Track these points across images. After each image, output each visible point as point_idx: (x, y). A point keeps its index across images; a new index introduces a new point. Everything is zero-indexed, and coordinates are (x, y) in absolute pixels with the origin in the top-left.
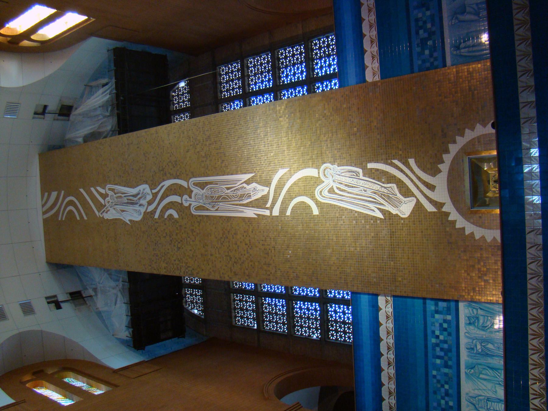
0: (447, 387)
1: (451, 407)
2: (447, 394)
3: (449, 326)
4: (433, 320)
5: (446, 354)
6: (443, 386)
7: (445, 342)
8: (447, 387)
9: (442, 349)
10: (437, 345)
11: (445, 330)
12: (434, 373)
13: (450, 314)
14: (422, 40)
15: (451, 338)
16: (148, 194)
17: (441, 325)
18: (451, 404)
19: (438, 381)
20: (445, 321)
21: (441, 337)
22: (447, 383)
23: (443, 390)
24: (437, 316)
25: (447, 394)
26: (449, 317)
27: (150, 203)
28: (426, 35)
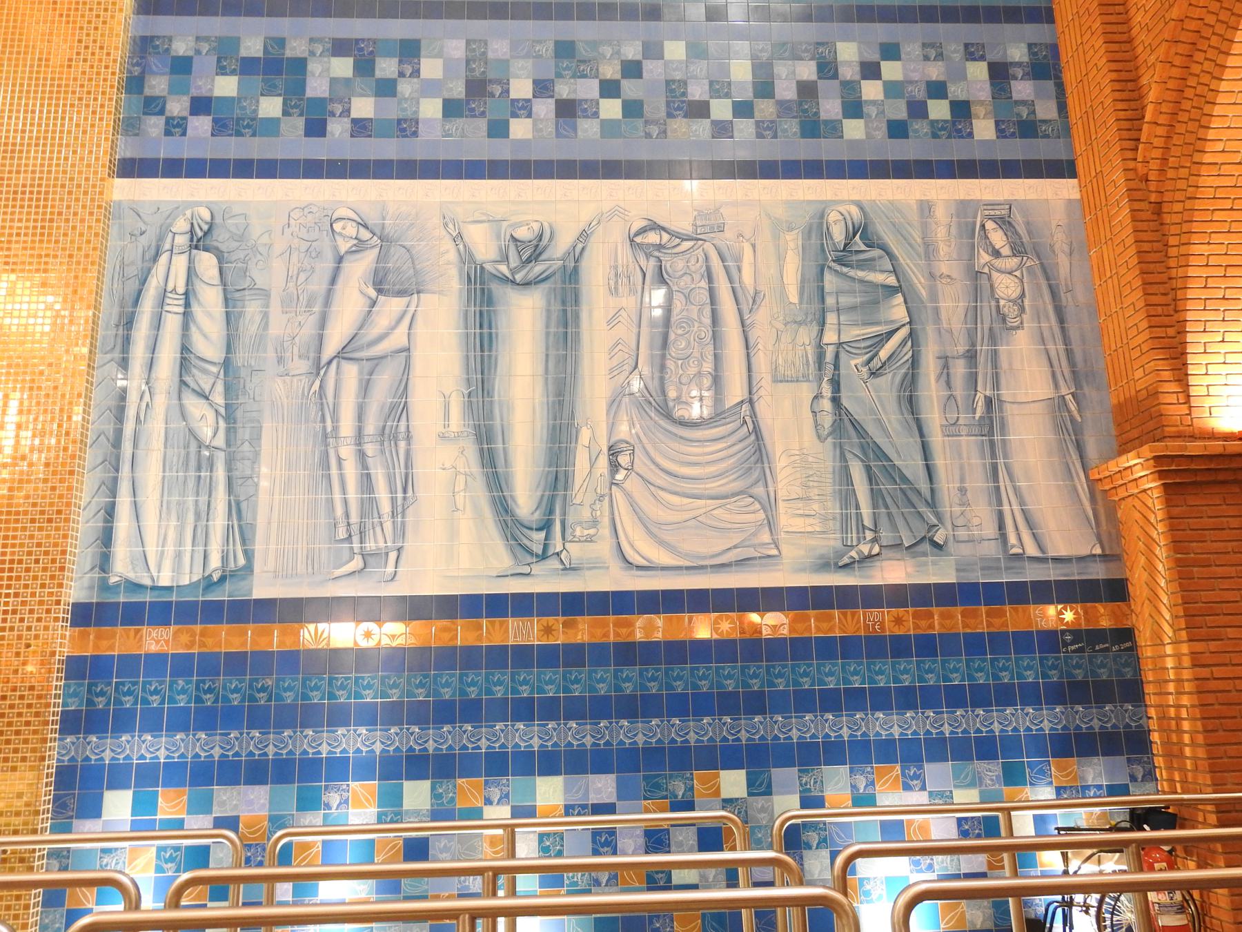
0: (611, 109)
1: (499, 129)
2: (567, 110)
3: (937, 129)
4: (955, 51)
5: (784, 107)
6: (610, 89)
7: (854, 108)
8: (611, 109)
9: (807, 90)
10: (828, 68)
11: (918, 109)
13: (1001, 133)
15: (881, 133)
17: (937, 90)
18: (520, 129)
19: (632, 70)
20: (962, 110)
21: (871, 90)
22: (633, 109)
23: (588, 89)
24: (978, 71)
25: (567, 110)
26: (984, 129)
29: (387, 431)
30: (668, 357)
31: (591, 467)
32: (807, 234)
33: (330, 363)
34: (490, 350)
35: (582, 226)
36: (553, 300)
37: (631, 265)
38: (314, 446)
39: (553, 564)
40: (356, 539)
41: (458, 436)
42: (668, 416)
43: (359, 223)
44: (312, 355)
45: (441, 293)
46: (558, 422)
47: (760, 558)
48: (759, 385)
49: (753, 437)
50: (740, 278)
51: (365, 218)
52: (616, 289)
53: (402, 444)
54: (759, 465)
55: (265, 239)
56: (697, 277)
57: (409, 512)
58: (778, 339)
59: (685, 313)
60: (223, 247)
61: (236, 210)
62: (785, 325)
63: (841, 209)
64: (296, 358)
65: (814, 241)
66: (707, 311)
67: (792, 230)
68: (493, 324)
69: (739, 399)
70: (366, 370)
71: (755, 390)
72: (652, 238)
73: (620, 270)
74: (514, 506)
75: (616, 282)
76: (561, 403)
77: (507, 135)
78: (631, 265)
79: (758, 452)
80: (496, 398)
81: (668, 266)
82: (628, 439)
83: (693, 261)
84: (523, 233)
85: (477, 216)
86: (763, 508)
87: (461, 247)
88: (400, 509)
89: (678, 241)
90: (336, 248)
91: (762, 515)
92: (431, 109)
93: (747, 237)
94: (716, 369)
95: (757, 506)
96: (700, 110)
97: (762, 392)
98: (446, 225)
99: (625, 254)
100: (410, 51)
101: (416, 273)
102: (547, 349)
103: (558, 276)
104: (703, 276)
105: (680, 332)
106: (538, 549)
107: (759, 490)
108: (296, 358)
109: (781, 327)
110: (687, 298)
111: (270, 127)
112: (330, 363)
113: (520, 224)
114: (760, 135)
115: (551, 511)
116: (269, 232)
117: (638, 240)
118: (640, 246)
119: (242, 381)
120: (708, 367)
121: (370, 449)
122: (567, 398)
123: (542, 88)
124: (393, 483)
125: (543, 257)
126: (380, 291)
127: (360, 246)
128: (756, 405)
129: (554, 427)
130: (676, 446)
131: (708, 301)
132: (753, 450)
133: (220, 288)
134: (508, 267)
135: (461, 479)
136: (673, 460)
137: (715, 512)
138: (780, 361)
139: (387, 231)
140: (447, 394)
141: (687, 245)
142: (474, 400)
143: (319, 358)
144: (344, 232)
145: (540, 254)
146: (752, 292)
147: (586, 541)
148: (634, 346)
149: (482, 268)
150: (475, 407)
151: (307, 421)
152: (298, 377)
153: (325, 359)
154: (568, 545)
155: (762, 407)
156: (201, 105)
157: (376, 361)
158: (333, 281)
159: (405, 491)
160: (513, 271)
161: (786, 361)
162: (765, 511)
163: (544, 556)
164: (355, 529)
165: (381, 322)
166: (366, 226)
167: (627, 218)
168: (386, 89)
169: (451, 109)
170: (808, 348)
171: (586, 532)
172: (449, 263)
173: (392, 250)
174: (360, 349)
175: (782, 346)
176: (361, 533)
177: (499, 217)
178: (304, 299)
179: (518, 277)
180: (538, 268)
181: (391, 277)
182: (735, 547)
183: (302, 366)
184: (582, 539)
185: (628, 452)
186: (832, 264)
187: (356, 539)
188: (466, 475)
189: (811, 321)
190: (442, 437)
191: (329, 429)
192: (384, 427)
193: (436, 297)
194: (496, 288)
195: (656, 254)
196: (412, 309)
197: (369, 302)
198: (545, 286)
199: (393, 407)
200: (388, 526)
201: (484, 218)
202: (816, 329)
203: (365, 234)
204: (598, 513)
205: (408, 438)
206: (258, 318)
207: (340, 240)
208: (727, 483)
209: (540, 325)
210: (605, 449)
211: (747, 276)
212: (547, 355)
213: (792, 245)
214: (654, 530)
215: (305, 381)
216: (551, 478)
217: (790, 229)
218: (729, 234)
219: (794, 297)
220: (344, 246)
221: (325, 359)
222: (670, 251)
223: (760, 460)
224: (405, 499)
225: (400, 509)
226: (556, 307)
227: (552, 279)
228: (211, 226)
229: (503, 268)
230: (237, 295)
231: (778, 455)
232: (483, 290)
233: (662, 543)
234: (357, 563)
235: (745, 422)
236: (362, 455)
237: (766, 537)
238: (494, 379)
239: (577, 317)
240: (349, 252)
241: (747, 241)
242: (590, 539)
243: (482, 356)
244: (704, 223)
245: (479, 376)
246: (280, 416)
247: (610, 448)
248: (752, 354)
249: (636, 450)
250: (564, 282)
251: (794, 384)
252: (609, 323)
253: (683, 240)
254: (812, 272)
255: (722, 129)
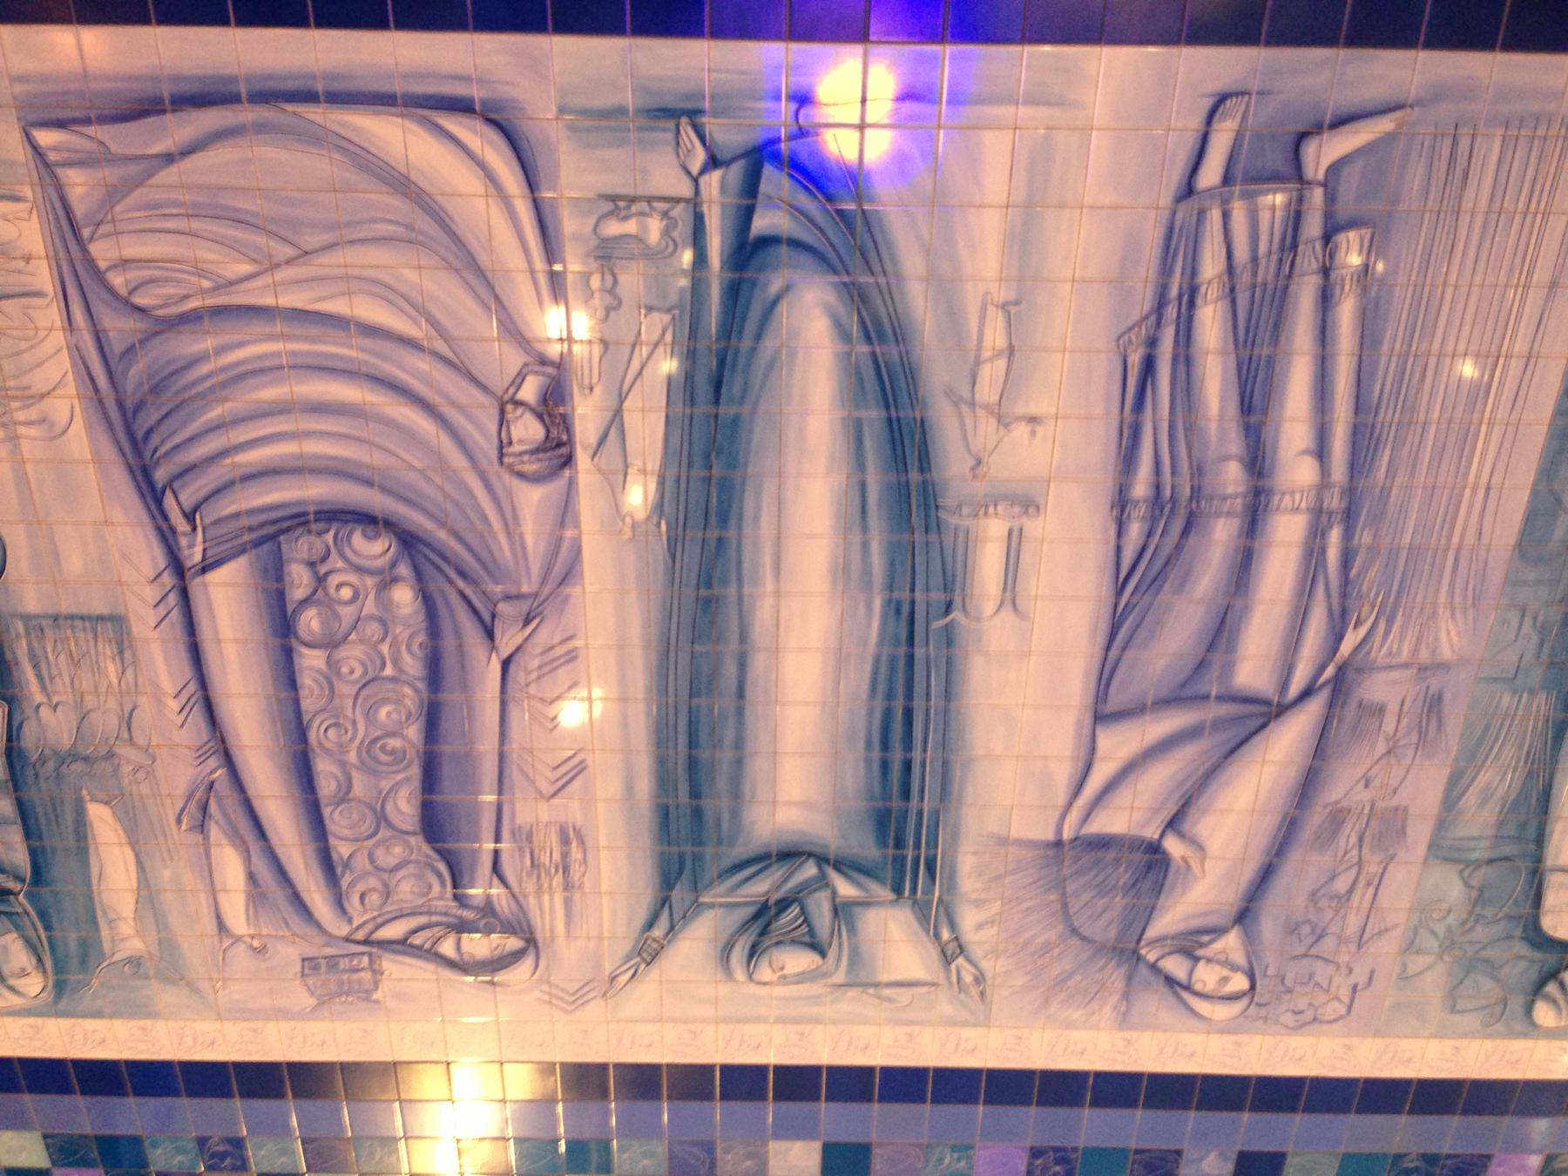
29: (1178, 526)
30: (421, 685)
31: (618, 414)
32: (89, 952)
33: (1306, 694)
34: (887, 715)
35: (655, 973)
36: (726, 818)
37: (530, 886)
38: (1385, 493)
39: (730, 135)
40: (1313, 226)
41: (984, 507)
42: (409, 541)
43: (1188, 988)
44: (1350, 712)
45: (1003, 841)
46: (713, 534)
47: (87, 121)
48: (162, 610)
49: (160, 475)
50: (248, 860)
51: (1172, 999)
52: (565, 841)
53: (1141, 488)
54: (130, 404)
55: (1416, 963)
56: (361, 862)
57: (1143, 300)
58: (128, 721)
59: (386, 784)
60: (1522, 949)
61: (1471, 1021)
62: (110, 755)
63: (17, 1001)
64: (1393, 708)
65: (71, 938)
66: (326, 787)
67: (129, 960)
68: (876, 766)
69: (216, 576)
70: (1215, 671)
71: (173, 599)
72: (478, 945)
73: (558, 880)
74: (842, 310)
75: (565, 856)
76: (707, 579)
77: (827, 1148)
78: (530, 886)
79: (140, 434)
80: (877, 603)
81: (436, 888)
82: (519, 486)
83: (374, 898)
84: (798, 961)
85: (904, 996)
86: (99, 275)
87: (946, 935)
88: (1171, 312)
89: (417, 940)
90: (1250, 939)
91: (102, 252)
93: (240, 948)
94: (287, 656)
95: (117, 280)
97: (151, 593)
98: (979, 979)
99: (547, 912)
101: (1060, 885)
102: (740, 712)
103: (712, 870)
104: (347, 865)
105: (394, 743)
106: (775, 181)
107: (119, 327)
108: (1393, 708)
109: (125, 751)
110: (382, 819)
112: (1306, 694)
113: (802, 978)
114: (238, 1143)
115: (735, 294)
116: (1404, 977)
117: (513, 943)
118: (509, 928)
119: (1545, 657)
120: (311, 661)
121: (1232, 477)
122: (690, 592)
124: (1181, 385)
125: (749, 911)
126: (1154, 849)
127: (1190, 944)
128: (162, 562)
129: (724, 521)
130: (378, 459)
131: (326, 811)
132: (155, 440)
133: (1549, 862)
134: (834, 893)
135: (987, 390)
136: (391, 424)
137: (246, 268)
138: (112, 669)
139: (1123, 971)
140: (1007, 613)
141: (394, 931)
142: (937, 596)
143: (1331, 704)
144: (1225, 972)
145: (756, 917)
146: (215, 832)
147: (633, 200)
148: (514, 714)
149: (898, 889)
150: (936, 579)
151: (1394, 552)
152: (1394, 661)
153: (1314, 708)
154: (684, 189)
155: (146, 555)
157: (1188, 692)
158: (1266, 874)
159: (1149, 366)
160: (822, 882)
161: (98, 669)
162: (91, 263)
163: (762, 154)
164: (1309, 259)
165: (1160, 778)
166: (1170, 981)
167: (545, 988)
170: (38, 697)
171: (631, 227)
172: (979, 904)
173: (1113, 933)
174: (1218, 725)
175: (112, 703)
176: (1294, 246)
177: (851, 993)
178: (1348, 835)
179: (810, 870)
180: (761, 887)
181: (1123, 877)
182: (169, 158)
183: (1381, 688)
184: (643, 206)
185: (516, 448)
186: (11, 885)
187: (1313, 226)
188: (973, 404)
189: (43, 760)
190: (1029, 505)
191: (1335, 536)
192: (1186, 532)
193: (1015, 833)
194: (867, 848)
195: (468, 915)
196: (1074, 815)
197: (1186, 826)
198: (740, 851)
199: (1155, 582)
200: (1211, 266)
201: (887, 992)
202: (29, 738)
203: (1175, 966)
204: (595, 282)
205: (1121, 503)
206: (1470, 799)
207: (1239, 958)
208: (220, 350)
209: (757, 767)
210: (582, 458)
211: (231, 867)
212: (741, 694)
213: (126, 928)
214: (424, 223)
215: (1379, 654)
216: (733, 386)
217: (135, 962)
218: (289, 953)
219: (100, 817)
220: (1231, 942)
221: (1314, 708)
222: (434, 919)
223: (129, 414)
224: (1152, 342)
225: (1171, 312)
226: (716, 804)
227: (727, 863)
228: (1537, 990)
229: (845, 889)
230: (1508, 849)
231: (79, 424)
232: (899, 843)
233: (402, 184)
234: (1322, 154)
235: (190, 517)
236: (1258, 462)
237: (80, 185)
238: (881, 643)
239: (663, 780)
240: (1218, 931)
241: (238, 939)
242: (618, 204)
243: (909, 695)
244: (355, 976)
245: (919, 652)
246: (1463, 564)
247: (568, 461)
248: (192, 687)
249: (494, 455)
250: (698, 858)
251: (65, 608)
252: (582, 768)
253: (403, 942)
254: (61, 869)
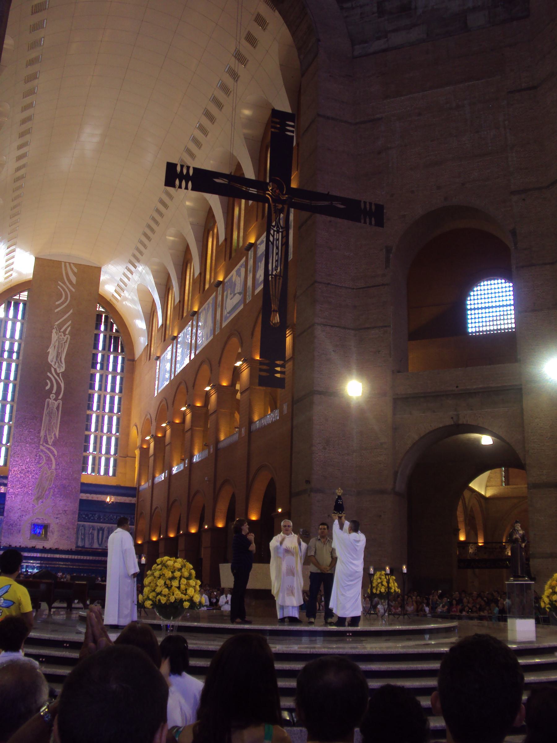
0: (107, 519)
1: (100, 520)
6: (107, 518)
8: (107, 519)
12: (111, 516)
14: (88, 515)
16: (60, 370)
18: (101, 520)
22: (108, 519)
25: (104, 519)
27: (55, 370)
28: (89, 517)
92: (96, 518)
96: (112, 519)
100: (95, 514)
111: (87, 519)
123: (103, 518)
156: (83, 517)
168: (93, 517)
169: (97, 519)
255: (114, 521)
